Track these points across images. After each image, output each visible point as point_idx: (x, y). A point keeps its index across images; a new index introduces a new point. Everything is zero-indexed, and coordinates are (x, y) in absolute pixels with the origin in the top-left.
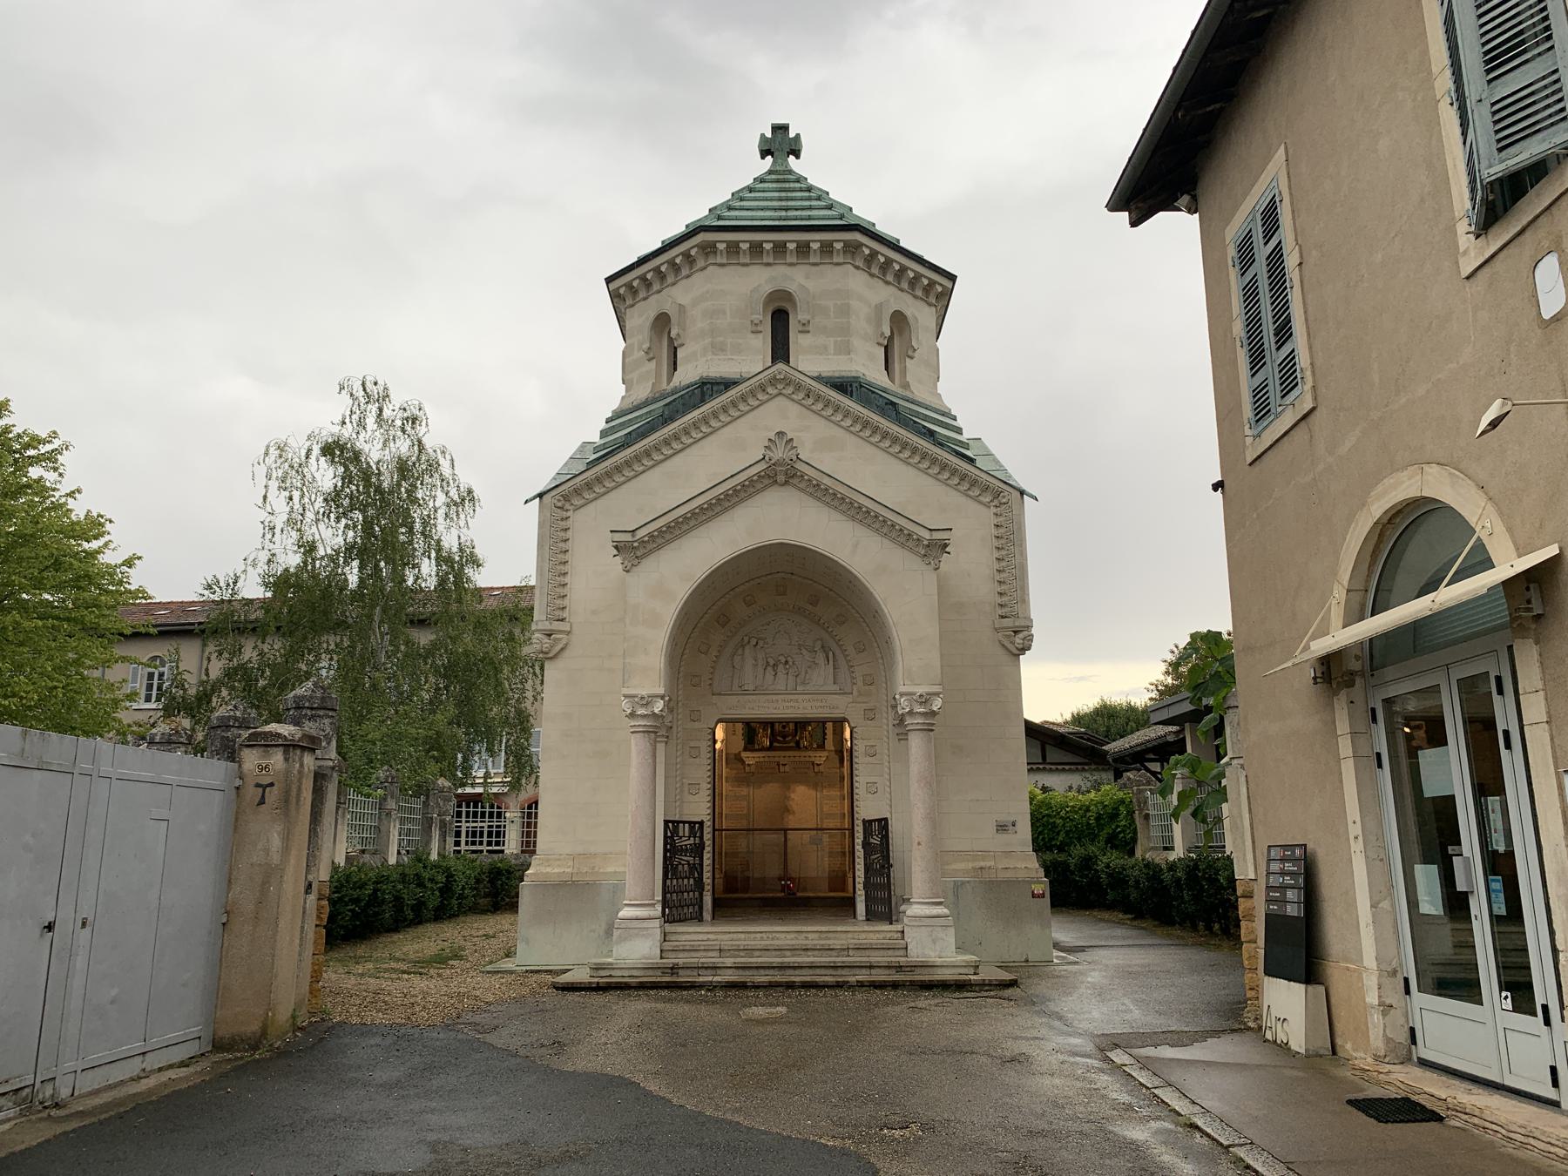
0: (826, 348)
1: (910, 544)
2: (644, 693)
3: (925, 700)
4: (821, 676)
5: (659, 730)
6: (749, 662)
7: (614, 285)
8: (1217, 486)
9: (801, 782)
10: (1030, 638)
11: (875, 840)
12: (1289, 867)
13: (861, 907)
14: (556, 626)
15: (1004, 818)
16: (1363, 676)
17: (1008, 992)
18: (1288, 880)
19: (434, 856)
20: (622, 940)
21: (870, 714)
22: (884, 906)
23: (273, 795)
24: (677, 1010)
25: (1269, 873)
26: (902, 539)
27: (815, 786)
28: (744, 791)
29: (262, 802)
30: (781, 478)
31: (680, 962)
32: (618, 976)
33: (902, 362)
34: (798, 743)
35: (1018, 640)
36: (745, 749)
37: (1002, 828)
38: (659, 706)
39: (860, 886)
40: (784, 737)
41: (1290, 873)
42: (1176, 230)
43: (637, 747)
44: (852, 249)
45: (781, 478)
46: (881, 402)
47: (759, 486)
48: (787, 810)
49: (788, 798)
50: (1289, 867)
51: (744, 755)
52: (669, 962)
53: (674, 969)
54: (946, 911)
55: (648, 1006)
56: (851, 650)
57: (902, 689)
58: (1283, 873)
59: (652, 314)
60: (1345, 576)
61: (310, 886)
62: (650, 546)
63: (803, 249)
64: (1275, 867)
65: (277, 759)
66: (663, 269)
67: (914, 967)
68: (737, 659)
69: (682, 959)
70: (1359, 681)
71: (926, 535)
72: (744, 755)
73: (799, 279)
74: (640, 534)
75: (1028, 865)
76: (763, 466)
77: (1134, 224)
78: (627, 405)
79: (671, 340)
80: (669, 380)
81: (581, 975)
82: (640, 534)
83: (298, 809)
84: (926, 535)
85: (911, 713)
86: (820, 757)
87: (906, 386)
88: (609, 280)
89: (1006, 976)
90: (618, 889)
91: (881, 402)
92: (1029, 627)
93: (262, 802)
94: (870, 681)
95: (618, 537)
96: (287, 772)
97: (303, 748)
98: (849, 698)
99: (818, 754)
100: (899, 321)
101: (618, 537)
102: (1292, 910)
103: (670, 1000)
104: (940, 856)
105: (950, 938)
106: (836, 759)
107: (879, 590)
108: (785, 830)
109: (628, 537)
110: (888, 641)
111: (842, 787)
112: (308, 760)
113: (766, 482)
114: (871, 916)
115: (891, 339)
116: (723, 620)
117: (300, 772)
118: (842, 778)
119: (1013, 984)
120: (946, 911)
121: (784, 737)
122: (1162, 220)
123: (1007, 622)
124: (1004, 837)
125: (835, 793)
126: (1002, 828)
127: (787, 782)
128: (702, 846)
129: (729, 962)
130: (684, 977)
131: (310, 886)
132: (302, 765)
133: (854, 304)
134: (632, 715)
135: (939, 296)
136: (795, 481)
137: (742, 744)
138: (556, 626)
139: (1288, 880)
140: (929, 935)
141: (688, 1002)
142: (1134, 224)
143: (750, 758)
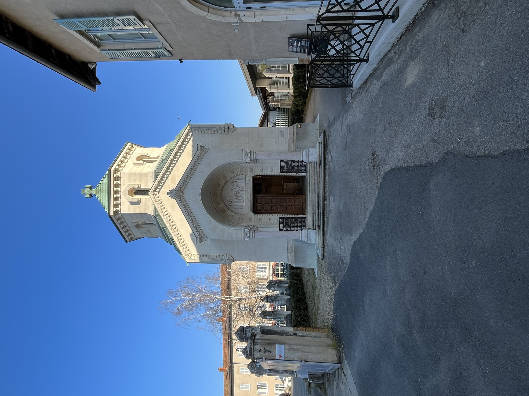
0: (146, 180)
1: (201, 156)
2: (243, 234)
3: (247, 154)
4: (241, 183)
5: (254, 229)
6: (236, 204)
7: (128, 240)
8: (181, 61)
10: (231, 125)
12: (295, 44)
13: (303, 174)
14: (224, 258)
15: (280, 134)
16: (236, 11)
17: (327, 134)
18: (299, 45)
19: (287, 285)
20: (310, 240)
21: (251, 170)
23: (268, 348)
24: (330, 226)
25: (297, 52)
26: (200, 159)
29: (270, 351)
30: (181, 194)
31: (317, 224)
33: (151, 158)
35: (231, 128)
37: (283, 135)
38: (247, 230)
41: (297, 45)
43: (258, 235)
45: (181, 194)
47: (183, 200)
50: (295, 44)
52: (317, 227)
53: (319, 226)
54: (305, 151)
55: (329, 235)
56: (233, 175)
57: (244, 160)
58: (297, 46)
59: (136, 229)
60: (203, 13)
61: (294, 334)
62: (201, 232)
63: (117, 185)
64: (295, 49)
65: (257, 347)
66: (122, 226)
67: (320, 160)
68: (235, 207)
69: (316, 224)
70: (238, 13)
71: (199, 152)
73: (124, 188)
74: (197, 235)
75: (292, 128)
77: (100, 83)
78: (163, 237)
79: (143, 224)
80: (155, 225)
81: (320, 252)
82: (197, 235)
83: (273, 340)
84: (199, 152)
85: (250, 158)
87: (158, 157)
88: (127, 242)
89: (323, 133)
90: (297, 241)
91: (162, 164)
92: (228, 125)
93: (270, 351)
94: (242, 170)
95: (198, 242)
96: (262, 344)
97: (254, 339)
98: (247, 176)
100: (139, 158)
101: (198, 242)
102: (308, 44)
103: (327, 228)
105: (312, 150)
107: (214, 166)
109: (198, 239)
110: (230, 164)
112: (258, 337)
113: (182, 198)
116: (224, 211)
117: (261, 339)
119: (325, 133)
120: (305, 151)
123: (226, 131)
124: (285, 134)
126: (283, 135)
128: (286, 218)
129: (317, 211)
131: (295, 334)
132: (259, 339)
133: (133, 171)
134: (249, 238)
136: (182, 190)
138: (224, 258)
139: (299, 45)
140: (312, 155)
141: (328, 223)
142: (100, 83)
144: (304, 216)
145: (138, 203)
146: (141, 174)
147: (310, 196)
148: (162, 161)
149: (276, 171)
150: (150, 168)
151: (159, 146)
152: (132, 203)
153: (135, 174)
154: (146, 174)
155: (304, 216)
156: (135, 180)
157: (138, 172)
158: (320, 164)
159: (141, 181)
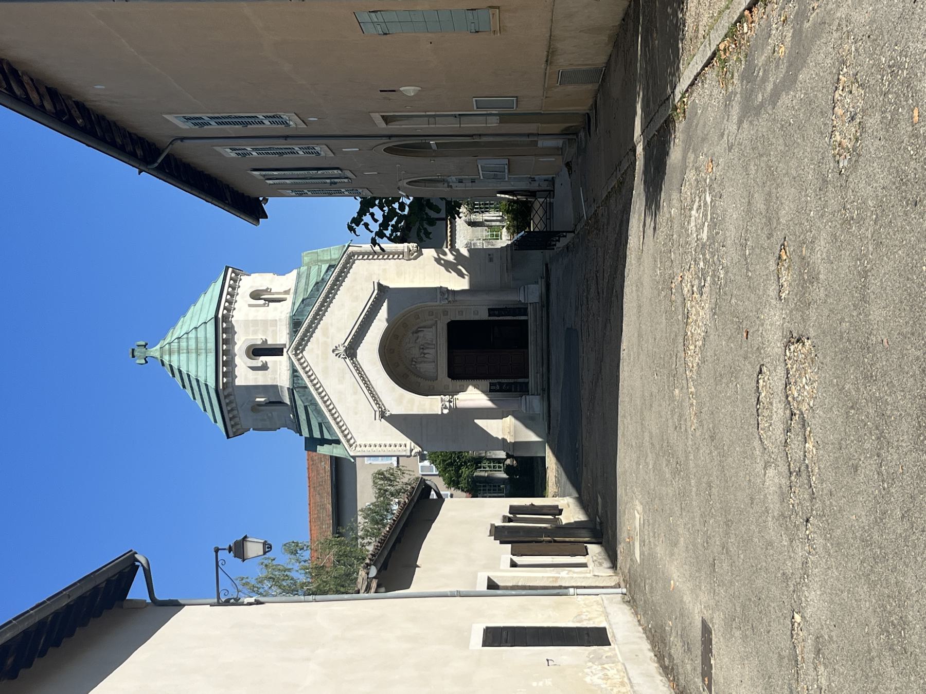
7: (231, 434)
11: (497, 312)
22: (523, 311)
32: (545, 410)
39: (515, 318)
42: (272, 206)
44: (226, 318)
46: (302, 306)
53: (543, 390)
63: (225, 342)
76: (347, 360)
82: (376, 408)
87: (287, 292)
88: (228, 437)
91: (302, 306)
104: (504, 288)
114: (526, 314)
115: (265, 300)
122: (266, 207)
128: (499, 383)
130: (546, 387)
135: (237, 275)
144: (526, 380)
145: (264, 367)
146: (265, 322)
147: (531, 348)
148: (303, 300)
149: (484, 315)
150: (282, 312)
151: (282, 272)
152: (253, 368)
153: (255, 322)
154: (274, 322)
155: (526, 380)
156: (255, 332)
157: (260, 318)
158: (543, 306)
159: (265, 332)
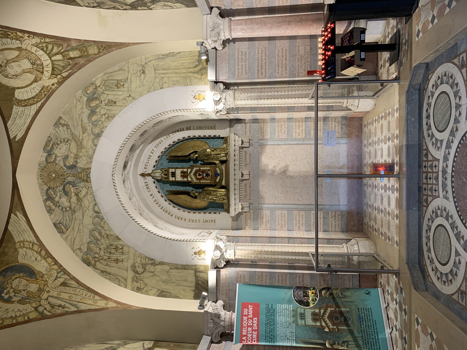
9: (259, 160)
27: (262, 146)
28: (266, 213)
34: (223, 162)
36: (228, 212)
40: (216, 175)
48: (284, 172)
49: (273, 171)
51: (233, 213)
72: (233, 213)
86: (235, 142)
99: (232, 143)
106: (238, 127)
108: (318, 176)
111: (264, 121)
118: (255, 121)
121: (216, 175)
125: (268, 128)
127: (258, 172)
137: (223, 214)
143: (236, 206)
